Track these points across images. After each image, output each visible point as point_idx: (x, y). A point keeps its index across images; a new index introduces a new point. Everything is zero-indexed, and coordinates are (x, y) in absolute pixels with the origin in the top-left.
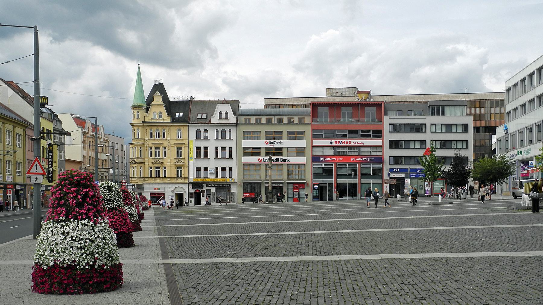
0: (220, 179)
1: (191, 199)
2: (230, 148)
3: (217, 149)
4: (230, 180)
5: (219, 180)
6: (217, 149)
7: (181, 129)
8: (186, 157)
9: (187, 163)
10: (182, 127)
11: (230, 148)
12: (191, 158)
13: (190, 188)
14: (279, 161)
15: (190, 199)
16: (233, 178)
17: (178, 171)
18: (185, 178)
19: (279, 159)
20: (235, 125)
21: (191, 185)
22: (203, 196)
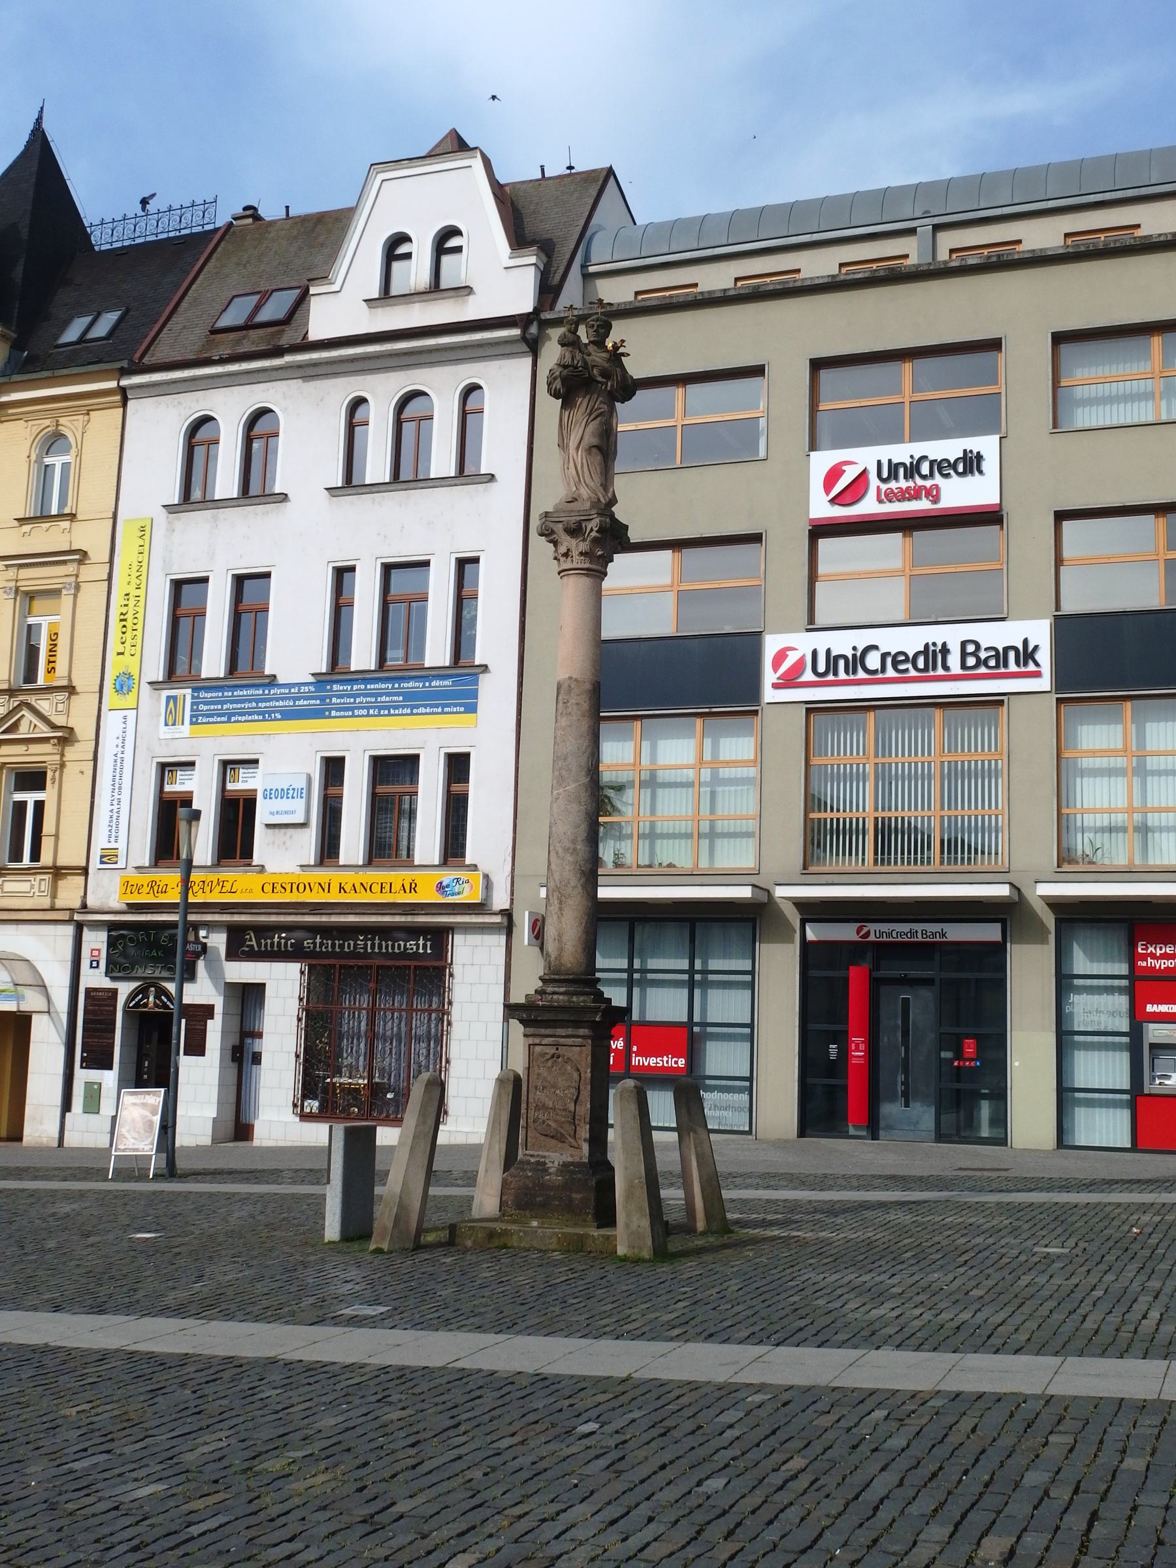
0: (349, 878)
1: (94, 1075)
2: (465, 565)
3: (342, 575)
4: (441, 887)
5: (341, 888)
6: (342, 575)
7: (70, 426)
8: (86, 679)
9: (84, 728)
10: (73, 411)
11: (465, 565)
12: (124, 685)
13: (94, 965)
14: (945, 667)
15: (82, 1076)
16: (474, 867)
17: (20, 807)
18: (58, 872)
19: (945, 650)
20: (516, 332)
21: (95, 941)
22: (197, 1047)
